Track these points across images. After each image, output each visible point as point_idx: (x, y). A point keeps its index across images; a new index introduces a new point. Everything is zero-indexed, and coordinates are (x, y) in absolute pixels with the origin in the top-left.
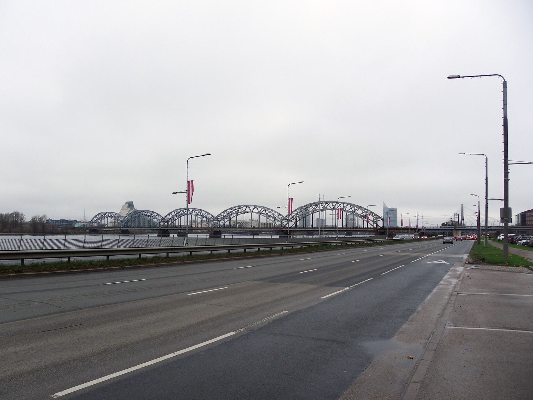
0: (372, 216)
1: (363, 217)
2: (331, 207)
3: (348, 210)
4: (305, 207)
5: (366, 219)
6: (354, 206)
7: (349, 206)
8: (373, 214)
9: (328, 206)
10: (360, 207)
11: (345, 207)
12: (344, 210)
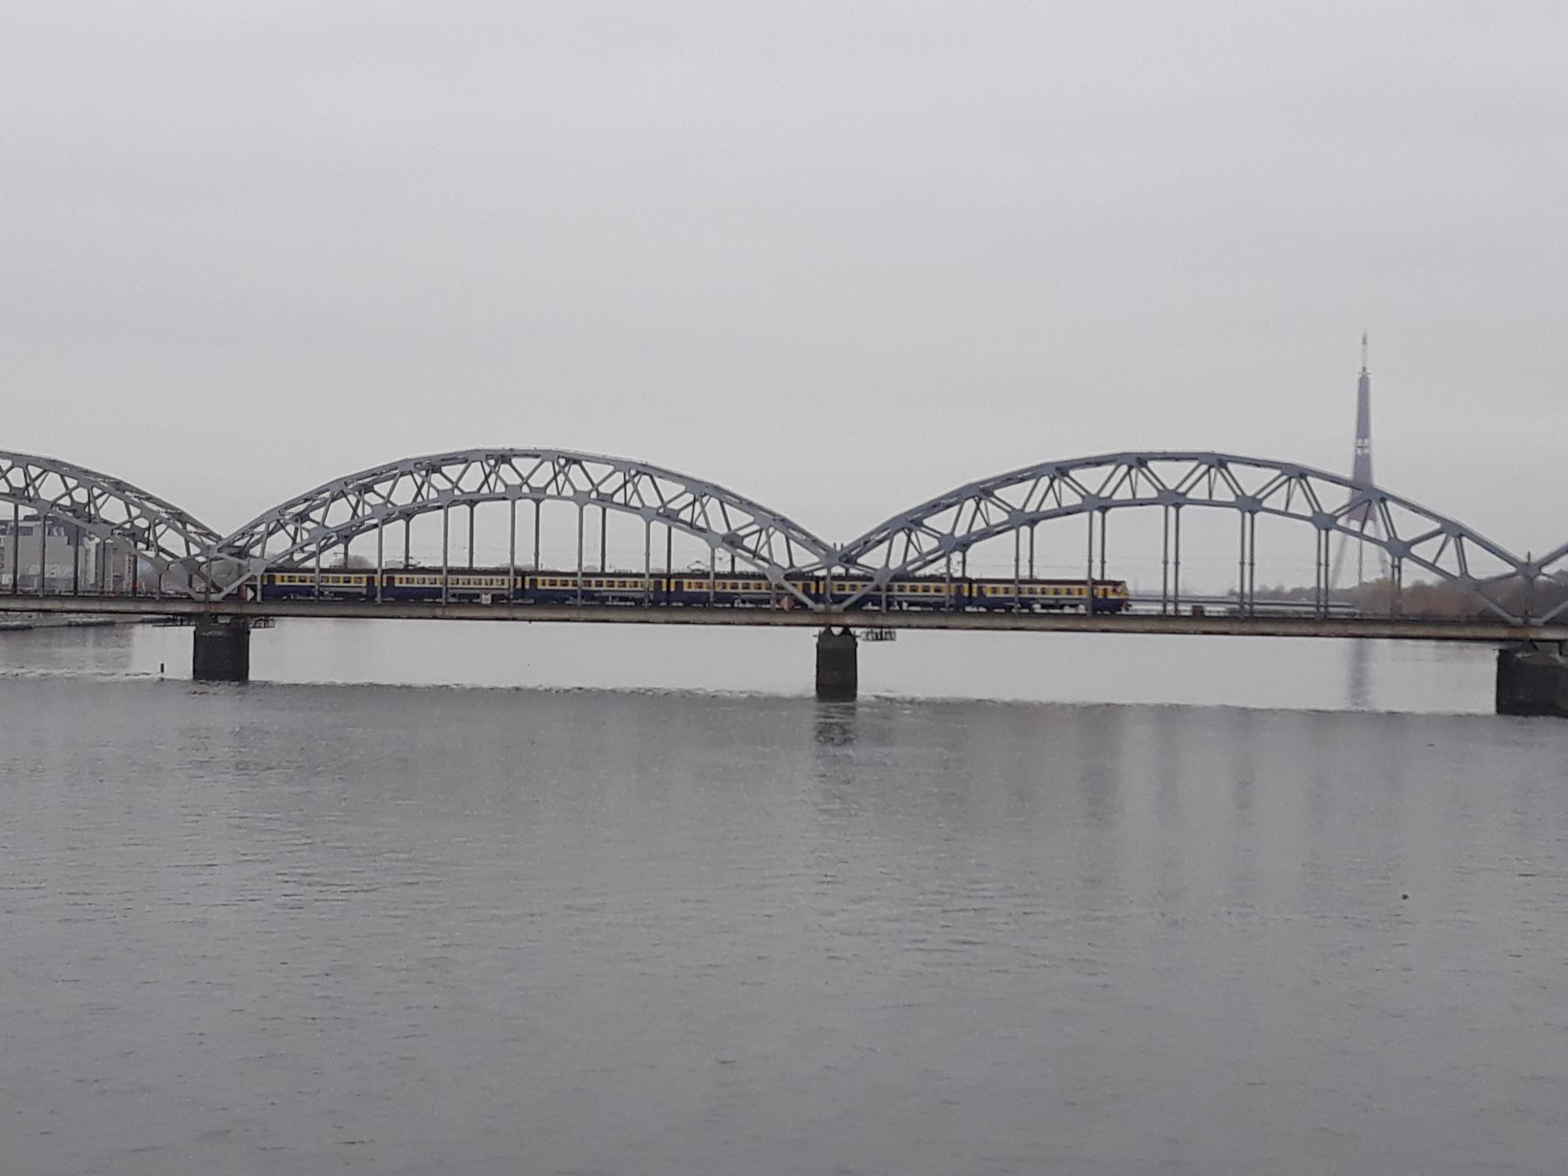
1: (133, 535)
3: (51, 499)
5: (147, 549)
6: (86, 477)
8: (189, 527)
9: (530, 476)
10: (119, 488)
11: (30, 482)
12: (29, 499)
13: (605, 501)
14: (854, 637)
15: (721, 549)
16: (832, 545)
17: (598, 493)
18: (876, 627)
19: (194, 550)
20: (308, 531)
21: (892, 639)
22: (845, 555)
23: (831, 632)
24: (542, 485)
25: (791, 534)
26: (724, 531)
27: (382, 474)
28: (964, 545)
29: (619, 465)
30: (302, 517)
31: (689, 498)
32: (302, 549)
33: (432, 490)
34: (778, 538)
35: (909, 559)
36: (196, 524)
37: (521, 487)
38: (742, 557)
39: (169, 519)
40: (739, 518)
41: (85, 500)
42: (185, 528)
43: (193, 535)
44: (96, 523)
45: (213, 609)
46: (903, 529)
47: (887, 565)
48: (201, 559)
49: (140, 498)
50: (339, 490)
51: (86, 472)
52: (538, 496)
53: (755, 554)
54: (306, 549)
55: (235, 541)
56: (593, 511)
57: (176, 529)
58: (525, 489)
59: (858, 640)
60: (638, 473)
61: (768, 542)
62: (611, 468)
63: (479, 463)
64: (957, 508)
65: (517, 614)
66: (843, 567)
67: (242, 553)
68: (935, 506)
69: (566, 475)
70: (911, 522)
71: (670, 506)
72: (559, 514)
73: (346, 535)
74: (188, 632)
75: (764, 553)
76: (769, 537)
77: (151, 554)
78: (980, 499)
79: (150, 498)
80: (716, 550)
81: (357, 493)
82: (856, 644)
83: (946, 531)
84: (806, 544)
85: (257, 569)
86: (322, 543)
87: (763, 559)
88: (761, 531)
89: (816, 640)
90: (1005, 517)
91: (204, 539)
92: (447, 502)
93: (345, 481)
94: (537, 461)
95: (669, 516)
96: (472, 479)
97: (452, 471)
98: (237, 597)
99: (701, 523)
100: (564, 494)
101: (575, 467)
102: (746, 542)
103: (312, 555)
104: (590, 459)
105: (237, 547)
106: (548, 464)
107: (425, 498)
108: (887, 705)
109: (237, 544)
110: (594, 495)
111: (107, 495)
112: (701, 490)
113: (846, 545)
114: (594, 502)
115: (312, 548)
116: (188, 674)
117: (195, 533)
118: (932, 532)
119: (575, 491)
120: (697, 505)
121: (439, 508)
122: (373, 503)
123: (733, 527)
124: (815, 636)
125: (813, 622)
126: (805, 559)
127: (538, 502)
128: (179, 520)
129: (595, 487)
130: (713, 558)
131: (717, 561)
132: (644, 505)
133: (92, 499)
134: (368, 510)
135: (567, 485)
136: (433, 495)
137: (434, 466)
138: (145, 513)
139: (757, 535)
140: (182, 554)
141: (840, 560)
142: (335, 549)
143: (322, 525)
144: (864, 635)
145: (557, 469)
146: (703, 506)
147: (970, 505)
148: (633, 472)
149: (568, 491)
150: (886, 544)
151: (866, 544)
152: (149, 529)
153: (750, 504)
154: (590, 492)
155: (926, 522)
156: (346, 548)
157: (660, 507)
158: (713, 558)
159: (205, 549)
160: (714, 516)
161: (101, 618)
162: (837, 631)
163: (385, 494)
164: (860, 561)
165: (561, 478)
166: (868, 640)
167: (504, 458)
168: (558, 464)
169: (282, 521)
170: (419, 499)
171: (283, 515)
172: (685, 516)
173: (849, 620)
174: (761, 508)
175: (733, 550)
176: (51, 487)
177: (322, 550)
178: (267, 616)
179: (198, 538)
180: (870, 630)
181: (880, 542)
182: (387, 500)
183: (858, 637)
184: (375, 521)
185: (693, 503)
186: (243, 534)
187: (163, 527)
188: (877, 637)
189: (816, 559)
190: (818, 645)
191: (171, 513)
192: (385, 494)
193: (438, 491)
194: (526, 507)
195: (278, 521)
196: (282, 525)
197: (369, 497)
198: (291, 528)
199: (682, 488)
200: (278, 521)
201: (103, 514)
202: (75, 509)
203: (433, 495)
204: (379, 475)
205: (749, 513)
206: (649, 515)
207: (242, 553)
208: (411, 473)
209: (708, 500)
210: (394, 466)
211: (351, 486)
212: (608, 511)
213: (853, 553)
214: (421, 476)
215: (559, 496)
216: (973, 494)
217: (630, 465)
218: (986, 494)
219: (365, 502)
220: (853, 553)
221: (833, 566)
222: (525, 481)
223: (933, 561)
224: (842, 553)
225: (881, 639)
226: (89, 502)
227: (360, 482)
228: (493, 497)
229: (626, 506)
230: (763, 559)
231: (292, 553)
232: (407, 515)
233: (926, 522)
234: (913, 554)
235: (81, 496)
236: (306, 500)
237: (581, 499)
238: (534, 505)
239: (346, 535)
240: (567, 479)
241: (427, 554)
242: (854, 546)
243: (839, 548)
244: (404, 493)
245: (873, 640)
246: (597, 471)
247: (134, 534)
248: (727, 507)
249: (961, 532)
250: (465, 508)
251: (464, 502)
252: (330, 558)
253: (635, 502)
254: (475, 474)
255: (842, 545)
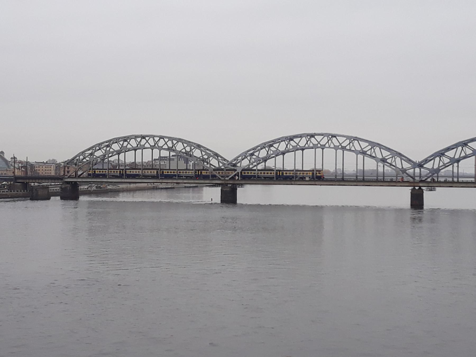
0: (217, 159)
2: (151, 145)
4: (107, 144)
6: (189, 144)
7: (180, 144)
8: (219, 158)
10: (199, 146)
12: (173, 150)
13: (344, 148)
14: (423, 190)
15: (380, 163)
16: (415, 161)
17: (342, 146)
18: (430, 187)
19: (221, 165)
20: (254, 159)
21: (435, 190)
22: (419, 164)
23: (415, 189)
24: (324, 144)
25: (402, 158)
26: (381, 157)
27: (276, 141)
28: (458, 161)
29: (348, 137)
30: (252, 155)
31: (370, 147)
32: (252, 164)
33: (291, 146)
34: (398, 159)
35: (440, 165)
36: (221, 157)
37: (317, 144)
38: (387, 165)
39: (213, 156)
40: (385, 153)
41: (189, 150)
42: (218, 158)
43: (220, 160)
44: (192, 157)
45: (227, 182)
46: (438, 156)
47: (433, 168)
48: (223, 167)
49: (205, 149)
50: (263, 146)
51: (190, 142)
52: (323, 147)
53: (391, 164)
54: (253, 164)
55: (232, 162)
56: (340, 152)
57: (215, 159)
58: (319, 145)
59: (424, 191)
60: (354, 140)
61: (395, 161)
62: (345, 138)
63: (305, 138)
64: (455, 149)
65: (317, 183)
66: (419, 168)
67: (235, 165)
68: (448, 149)
69: (331, 141)
70: (441, 154)
71: (364, 150)
72: (329, 153)
73: (265, 160)
74: (219, 189)
75: (394, 164)
76: (395, 159)
77: (208, 166)
78: (463, 146)
79: (208, 149)
80: (378, 163)
81: (268, 147)
82: (423, 192)
83: (452, 156)
84: (407, 161)
85: (239, 170)
86: (258, 162)
87: (393, 166)
88: (392, 157)
89: (410, 191)
90: (471, 152)
91: (223, 161)
92: (295, 149)
93: (265, 144)
94: (323, 137)
95: (364, 153)
96: (303, 142)
97: (297, 140)
98: (233, 178)
99: (374, 155)
100: (331, 146)
101: (334, 138)
102: (388, 161)
103: (255, 166)
104: (339, 136)
105: (233, 164)
106: (326, 138)
107: (289, 148)
108: (433, 211)
109: (233, 163)
110: (340, 147)
111: (195, 149)
112: (373, 145)
113: (420, 161)
114: (340, 149)
115: (255, 164)
116: (220, 202)
117: (221, 159)
118: (448, 157)
119: (334, 145)
120: (372, 149)
121: (293, 151)
122: (273, 150)
123: (384, 156)
124: (410, 190)
125: (409, 185)
126: (406, 165)
127: (323, 149)
128: (216, 156)
129: (341, 144)
130: (377, 166)
131: (379, 166)
132: (355, 150)
133: (191, 150)
134: (272, 152)
135: (332, 144)
136: (291, 147)
137: (291, 139)
138: (207, 154)
139: (391, 159)
140: (217, 166)
141: (418, 166)
142: (262, 164)
143: (258, 157)
144: (426, 189)
145: (329, 139)
146: (374, 150)
147: (460, 148)
148: (352, 140)
149: (332, 146)
150: (433, 161)
151: (426, 161)
152: (207, 158)
153: (389, 149)
154: (339, 146)
155: (446, 154)
156: (265, 164)
157: (361, 150)
158: (377, 166)
159: (224, 164)
160: (378, 153)
161: (194, 185)
162: (417, 188)
163: (277, 147)
164: (425, 166)
165: (330, 142)
166: (427, 191)
167: (312, 136)
168: (329, 137)
169: (246, 156)
170: (287, 149)
171: (246, 154)
172: (369, 153)
173: (421, 185)
174: (392, 150)
175: (383, 162)
176: (179, 147)
177: (258, 164)
178: (242, 184)
179: (222, 161)
180: (428, 188)
181: (431, 160)
182: (277, 149)
183: (424, 190)
184: (273, 156)
185: (371, 149)
186: (235, 160)
187: (211, 158)
188: (429, 189)
189: (410, 166)
190: (411, 193)
191: (214, 154)
192: (277, 147)
193: (293, 146)
194: (319, 151)
195: (245, 156)
196: (246, 157)
197: (272, 148)
198: (249, 158)
199: (367, 144)
200: (245, 156)
201: (195, 154)
202: (186, 153)
203: (291, 147)
204: (274, 142)
205: (389, 152)
206: (357, 152)
207: (235, 165)
208: (284, 141)
209: (376, 148)
210: (279, 139)
211: (266, 145)
212: (344, 151)
213: (422, 164)
214: (288, 142)
215: (329, 147)
216: (460, 145)
217: (352, 137)
218: (465, 145)
219: (271, 150)
220: (422, 164)
221: (416, 168)
222: (319, 143)
223: (448, 166)
224: (419, 163)
225: (431, 190)
226: (190, 151)
227: (269, 144)
228: (309, 148)
229: (350, 150)
230: (393, 166)
231: (249, 165)
232: (283, 153)
233: (446, 154)
234: (441, 164)
235: (188, 149)
236: (253, 149)
237: (336, 148)
238: (321, 150)
239: (265, 160)
240: (332, 142)
241: (289, 166)
242: (422, 162)
243: (417, 162)
244: (282, 146)
245: (429, 191)
246: (341, 139)
247: (203, 160)
248: (382, 150)
249: (457, 157)
250: (301, 151)
251: (300, 149)
252: (260, 167)
253: (353, 149)
254: (304, 140)
255: (419, 161)
